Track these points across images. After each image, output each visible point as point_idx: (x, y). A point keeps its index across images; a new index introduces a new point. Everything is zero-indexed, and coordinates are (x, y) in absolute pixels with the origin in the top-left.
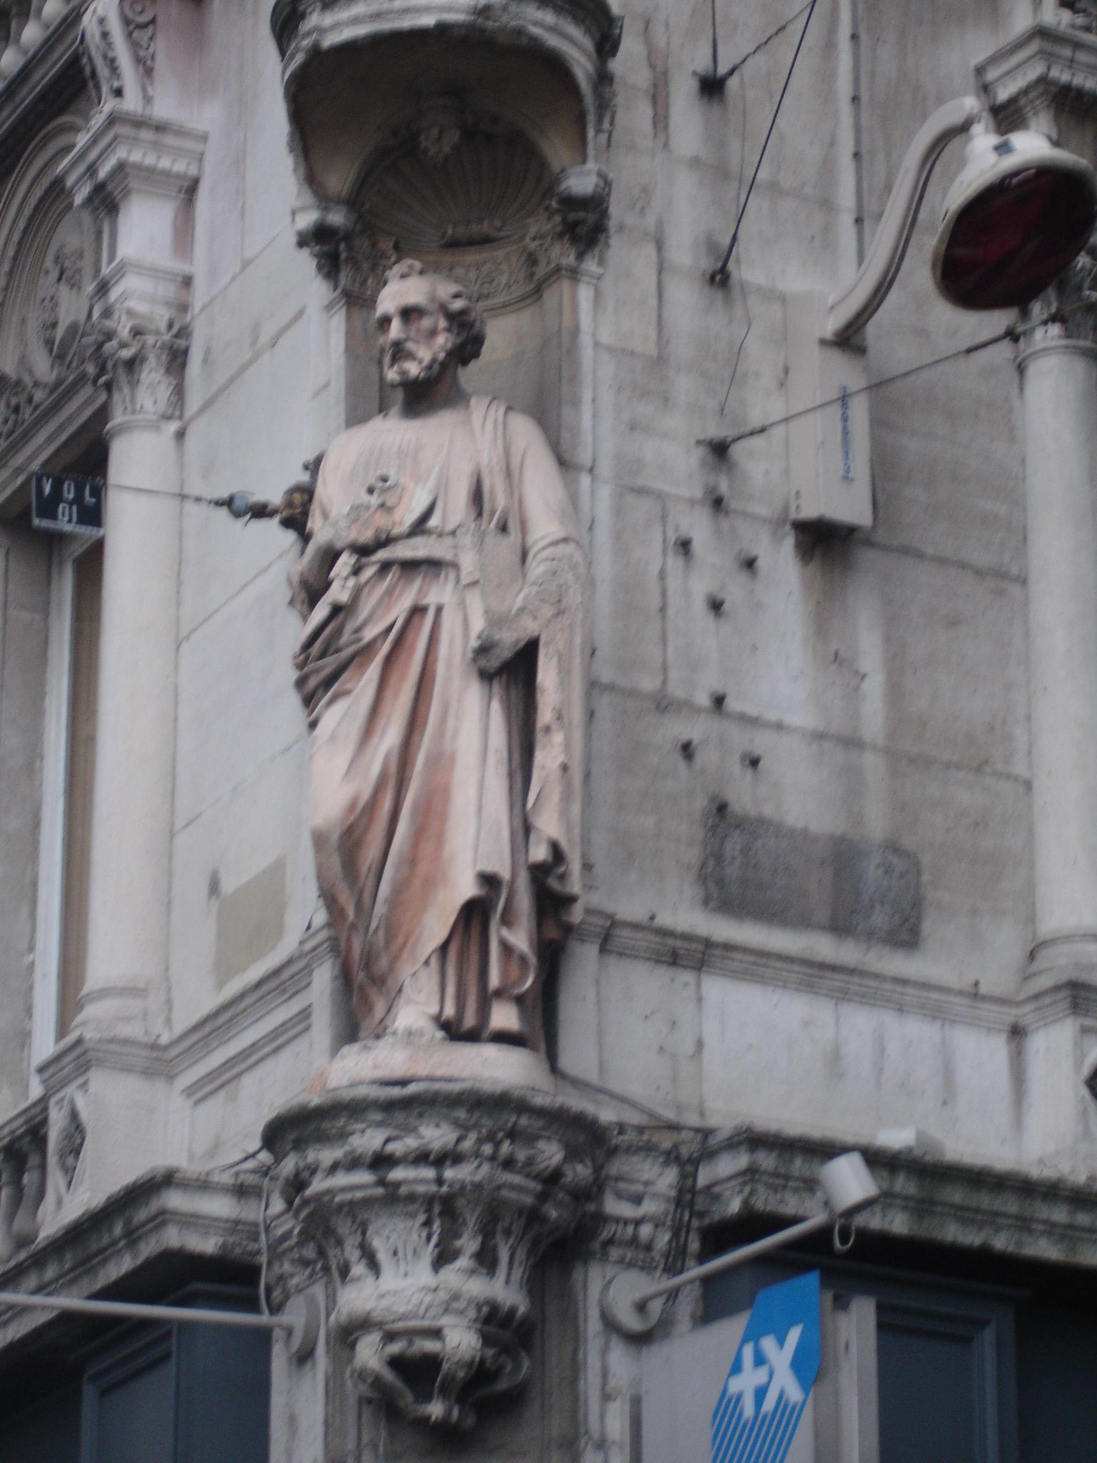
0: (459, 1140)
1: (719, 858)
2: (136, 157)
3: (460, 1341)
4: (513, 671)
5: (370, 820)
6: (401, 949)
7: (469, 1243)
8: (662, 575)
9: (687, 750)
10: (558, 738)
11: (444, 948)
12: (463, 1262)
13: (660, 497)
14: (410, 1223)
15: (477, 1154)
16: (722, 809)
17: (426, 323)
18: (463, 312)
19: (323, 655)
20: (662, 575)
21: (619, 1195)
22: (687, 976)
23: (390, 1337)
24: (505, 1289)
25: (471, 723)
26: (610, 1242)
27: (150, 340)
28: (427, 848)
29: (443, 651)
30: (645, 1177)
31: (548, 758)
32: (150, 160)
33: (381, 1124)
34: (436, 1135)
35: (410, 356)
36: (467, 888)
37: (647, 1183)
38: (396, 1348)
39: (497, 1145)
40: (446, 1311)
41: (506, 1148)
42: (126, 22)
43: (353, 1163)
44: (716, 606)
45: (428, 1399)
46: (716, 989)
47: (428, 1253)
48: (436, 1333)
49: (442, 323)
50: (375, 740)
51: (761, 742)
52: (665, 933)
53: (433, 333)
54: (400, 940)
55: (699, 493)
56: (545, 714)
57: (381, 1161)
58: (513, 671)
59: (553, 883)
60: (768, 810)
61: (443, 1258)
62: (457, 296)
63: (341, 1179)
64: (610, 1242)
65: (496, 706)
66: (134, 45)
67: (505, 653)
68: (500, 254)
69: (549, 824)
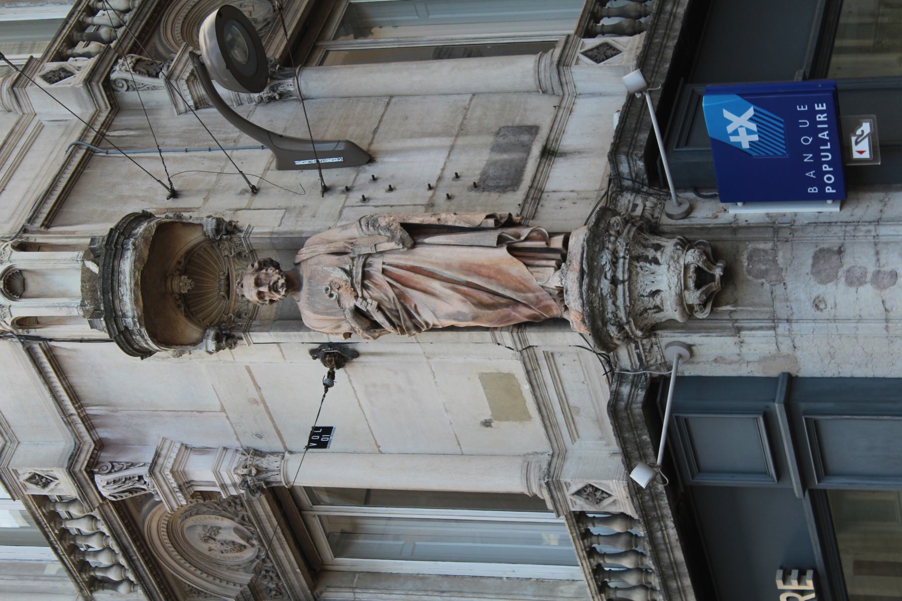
0: (608, 248)
1: (497, 187)
2: (170, 466)
3: (692, 257)
4: (415, 233)
5: (470, 296)
6: (525, 286)
7: (651, 253)
8: (375, 206)
9: (449, 197)
10: (443, 216)
11: (527, 265)
12: (658, 255)
13: (343, 207)
14: (640, 275)
15: (614, 243)
16: (475, 186)
17: (262, 276)
18: (260, 263)
19: (398, 318)
20: (375, 206)
21: (633, 210)
22: (545, 195)
23: (686, 287)
24: (669, 245)
25: (434, 253)
26: (652, 216)
27: (249, 463)
28: (484, 271)
29: (402, 262)
30: (627, 202)
31: (450, 220)
32: (172, 461)
33: (599, 282)
34: (605, 258)
35: (276, 282)
36: (503, 251)
37: (629, 201)
38: (691, 284)
39: (610, 235)
40: (678, 262)
41: (612, 232)
42: (110, 472)
43: (614, 293)
44: (391, 189)
45: (713, 276)
46: (550, 186)
47: (654, 267)
48: (686, 267)
49: (264, 271)
50: (437, 292)
51: (449, 174)
52: (525, 201)
53: (267, 274)
54: (522, 287)
55: (344, 196)
56: (433, 220)
57: (614, 282)
58: (415, 233)
59: (503, 221)
60: (478, 172)
61: (656, 261)
62: (253, 265)
63: (620, 302)
64: (652, 216)
65: (427, 240)
66: (120, 470)
67: (406, 235)
68: (234, 273)
69: (478, 218)
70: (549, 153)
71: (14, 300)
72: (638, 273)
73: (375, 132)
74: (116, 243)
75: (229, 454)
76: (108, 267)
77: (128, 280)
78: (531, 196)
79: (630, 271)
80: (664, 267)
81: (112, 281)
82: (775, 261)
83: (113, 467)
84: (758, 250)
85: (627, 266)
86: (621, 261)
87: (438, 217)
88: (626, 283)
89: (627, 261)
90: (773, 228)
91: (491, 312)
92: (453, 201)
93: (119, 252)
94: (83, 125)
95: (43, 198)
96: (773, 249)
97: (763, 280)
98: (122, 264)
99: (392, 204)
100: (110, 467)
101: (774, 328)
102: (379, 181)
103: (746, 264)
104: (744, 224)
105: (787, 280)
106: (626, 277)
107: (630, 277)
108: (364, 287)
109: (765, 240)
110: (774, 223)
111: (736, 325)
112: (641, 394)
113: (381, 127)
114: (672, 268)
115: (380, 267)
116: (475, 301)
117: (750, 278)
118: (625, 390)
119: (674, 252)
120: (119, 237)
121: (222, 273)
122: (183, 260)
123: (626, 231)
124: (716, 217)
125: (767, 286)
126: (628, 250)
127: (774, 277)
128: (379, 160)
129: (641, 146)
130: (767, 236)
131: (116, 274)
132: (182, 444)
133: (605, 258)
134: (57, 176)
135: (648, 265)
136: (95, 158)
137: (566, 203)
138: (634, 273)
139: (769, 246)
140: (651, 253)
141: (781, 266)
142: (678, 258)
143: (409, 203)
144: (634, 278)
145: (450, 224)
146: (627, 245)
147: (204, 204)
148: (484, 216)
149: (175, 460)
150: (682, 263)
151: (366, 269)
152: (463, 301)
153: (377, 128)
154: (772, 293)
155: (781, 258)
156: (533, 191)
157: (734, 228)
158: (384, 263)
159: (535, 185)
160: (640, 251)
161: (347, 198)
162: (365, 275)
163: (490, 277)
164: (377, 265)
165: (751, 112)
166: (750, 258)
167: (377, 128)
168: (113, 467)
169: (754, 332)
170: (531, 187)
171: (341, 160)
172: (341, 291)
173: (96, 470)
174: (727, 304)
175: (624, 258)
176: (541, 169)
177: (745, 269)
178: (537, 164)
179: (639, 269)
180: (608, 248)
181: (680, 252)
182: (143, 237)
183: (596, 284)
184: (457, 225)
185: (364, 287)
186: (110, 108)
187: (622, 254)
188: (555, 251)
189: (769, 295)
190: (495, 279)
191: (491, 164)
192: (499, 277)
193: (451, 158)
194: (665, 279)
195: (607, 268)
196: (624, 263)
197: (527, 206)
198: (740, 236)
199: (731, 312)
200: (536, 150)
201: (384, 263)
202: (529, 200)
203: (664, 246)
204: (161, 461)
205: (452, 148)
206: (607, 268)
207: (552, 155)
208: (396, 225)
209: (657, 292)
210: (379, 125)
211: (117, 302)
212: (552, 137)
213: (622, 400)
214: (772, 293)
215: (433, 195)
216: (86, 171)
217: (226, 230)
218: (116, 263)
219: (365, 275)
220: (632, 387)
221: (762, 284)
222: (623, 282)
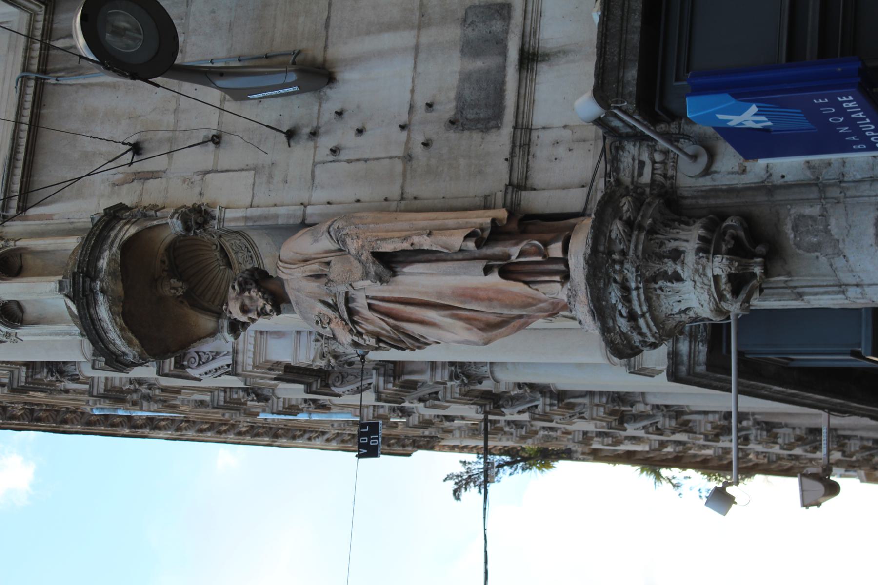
0: (615, 281)
1: (478, 121)
2: (250, 361)
3: (719, 266)
4: (389, 263)
5: (475, 320)
6: (533, 298)
7: (670, 267)
8: (349, 162)
9: (426, 144)
10: (416, 240)
11: (527, 283)
12: (679, 269)
13: (315, 164)
14: (662, 297)
15: (621, 271)
16: (452, 122)
17: (247, 302)
18: (240, 284)
19: (403, 342)
20: (349, 162)
21: (640, 174)
22: (534, 134)
23: (721, 297)
25: (416, 280)
26: (665, 176)
27: (325, 349)
28: (482, 294)
29: (387, 295)
30: (630, 161)
31: (425, 243)
32: (251, 355)
33: (614, 320)
34: (614, 295)
35: (263, 308)
36: (494, 279)
37: (633, 160)
38: (729, 296)
39: (614, 262)
40: (705, 275)
41: (616, 257)
42: (199, 365)
43: (637, 328)
44: (360, 131)
45: (754, 275)
46: (539, 118)
47: (676, 285)
48: (716, 278)
49: (247, 294)
50: (437, 321)
51: (420, 103)
52: (512, 152)
53: (251, 298)
54: (530, 300)
55: (311, 144)
56: (406, 246)
57: (632, 317)
58: (389, 263)
59: (486, 234)
60: (452, 94)
61: (677, 278)
62: (233, 287)
63: (645, 330)
64: (665, 176)
65: (407, 269)
66: (208, 361)
67: (381, 268)
68: (228, 244)
69: (456, 240)
70: (529, 59)
71: (16, 327)
72: (658, 297)
73: (327, 26)
74: (84, 291)
75: (304, 338)
76: (86, 319)
77: (111, 327)
78: (518, 144)
79: (648, 300)
80: (689, 284)
81: (96, 330)
82: (827, 231)
83: (200, 359)
84: (804, 216)
85: (643, 297)
86: (634, 293)
87: (410, 241)
88: (648, 315)
89: (642, 290)
90: (817, 186)
91: (504, 329)
92: (435, 146)
93: (91, 298)
94: (22, 40)
95: (9, 169)
96: (822, 215)
97: (817, 254)
98: (98, 311)
99: (366, 156)
100: (197, 359)
101: (843, 292)
102: (346, 115)
103: (792, 236)
104: (781, 182)
105: (847, 252)
106: (645, 308)
107: (650, 307)
108: (354, 323)
109: (810, 202)
110: (818, 179)
111: (795, 291)
112: (703, 349)
113: (332, 15)
114: (698, 284)
115: (365, 302)
116: (482, 325)
117: (801, 252)
118: (684, 347)
119: (697, 263)
120: (84, 282)
121: (214, 247)
122: (166, 259)
123: (632, 246)
124: (744, 171)
125: (823, 259)
126: (640, 276)
127: (829, 251)
128: (339, 76)
129: (630, 93)
130: (812, 196)
131: (97, 323)
132: (256, 331)
133: (614, 295)
134: (14, 131)
135: (669, 284)
136: (48, 89)
137: (561, 151)
138: (654, 298)
139: (816, 210)
140: (670, 267)
141: (836, 237)
142: (704, 268)
143: (383, 155)
144: (655, 303)
145: (426, 248)
146: (637, 271)
147: (169, 164)
148: (462, 239)
149: (254, 353)
150: (710, 275)
151: (350, 305)
152: (468, 329)
153: (329, 17)
154: (831, 265)
155: (835, 226)
156: (519, 132)
157: (767, 188)
158: (367, 297)
159: (520, 121)
160: (656, 267)
161: (315, 147)
162: (351, 312)
163: (490, 300)
164: (361, 304)
165: (754, 109)
166: (795, 228)
167: (329, 17)
168: (200, 359)
169: (817, 297)
170: (515, 128)
171: (296, 88)
172: (332, 325)
173: (186, 363)
174: (779, 275)
175: (637, 288)
176: (523, 91)
177: (791, 242)
178: (517, 76)
179: (659, 292)
180: (615, 281)
181: (705, 260)
182: (110, 274)
183: (611, 324)
184: (434, 248)
185: (354, 323)
186: (44, 7)
187: (633, 285)
188: (555, 260)
189: (829, 267)
190: (497, 300)
191: (466, 77)
192: (500, 297)
193: (419, 70)
194: (693, 297)
195: (620, 306)
196: (638, 296)
197: (516, 160)
198: (779, 197)
199: (787, 281)
200: (513, 54)
201: (367, 297)
202: (517, 150)
203: (684, 252)
204: (240, 358)
205: (417, 49)
206: (620, 306)
207: (533, 60)
208: (366, 256)
209: (688, 309)
210: (329, 12)
211: (111, 346)
212: (528, 29)
213: (682, 363)
214: (831, 265)
215: (409, 138)
216: (44, 111)
217: (196, 223)
218: (92, 311)
219: (351, 312)
220: (690, 342)
221: (817, 257)
222: (643, 315)
